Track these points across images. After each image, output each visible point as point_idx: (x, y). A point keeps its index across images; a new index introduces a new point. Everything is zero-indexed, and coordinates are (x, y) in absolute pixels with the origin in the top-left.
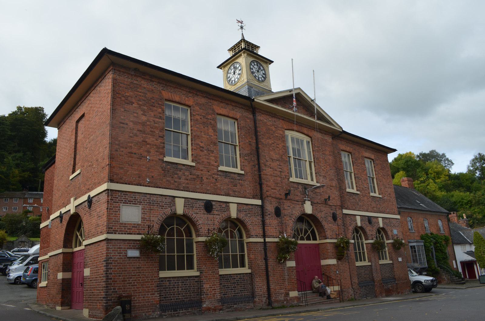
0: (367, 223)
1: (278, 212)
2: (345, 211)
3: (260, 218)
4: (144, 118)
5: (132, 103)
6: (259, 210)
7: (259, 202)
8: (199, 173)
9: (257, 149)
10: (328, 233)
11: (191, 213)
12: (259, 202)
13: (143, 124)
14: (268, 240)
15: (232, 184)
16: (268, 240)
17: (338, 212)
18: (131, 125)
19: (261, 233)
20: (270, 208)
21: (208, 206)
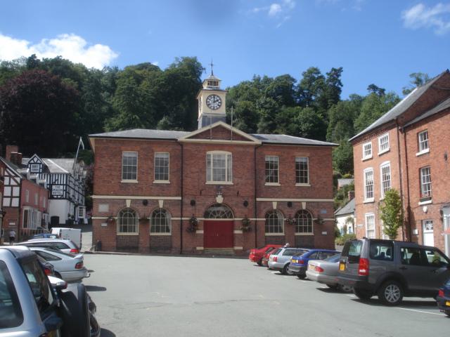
0: (286, 206)
1: (193, 203)
2: (258, 199)
3: (180, 207)
4: (110, 163)
5: (104, 157)
6: (180, 202)
7: (180, 198)
8: (140, 186)
9: (182, 167)
10: (237, 214)
11: (135, 206)
12: (180, 198)
13: (110, 166)
14: (183, 219)
15: (162, 190)
16: (183, 219)
17: (250, 201)
18: (104, 167)
19: (180, 214)
20: (187, 201)
21: (145, 203)
